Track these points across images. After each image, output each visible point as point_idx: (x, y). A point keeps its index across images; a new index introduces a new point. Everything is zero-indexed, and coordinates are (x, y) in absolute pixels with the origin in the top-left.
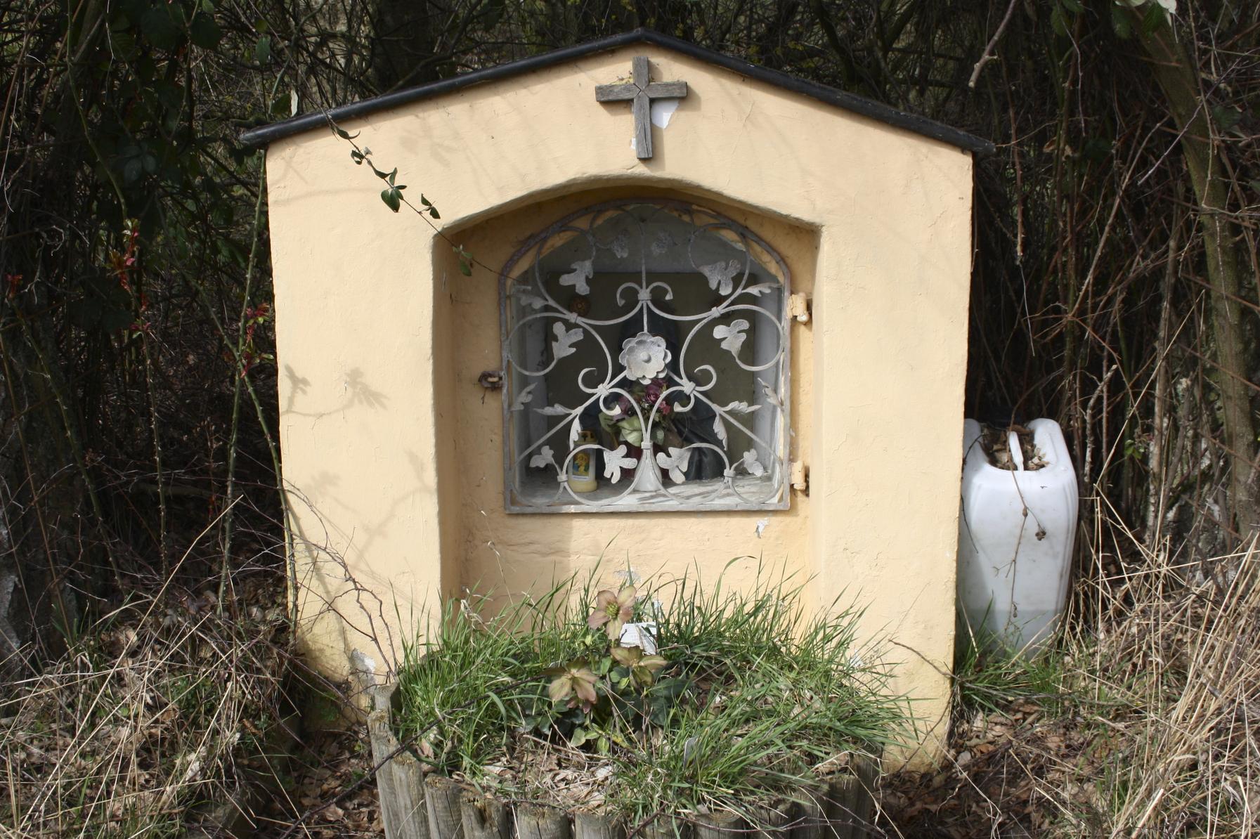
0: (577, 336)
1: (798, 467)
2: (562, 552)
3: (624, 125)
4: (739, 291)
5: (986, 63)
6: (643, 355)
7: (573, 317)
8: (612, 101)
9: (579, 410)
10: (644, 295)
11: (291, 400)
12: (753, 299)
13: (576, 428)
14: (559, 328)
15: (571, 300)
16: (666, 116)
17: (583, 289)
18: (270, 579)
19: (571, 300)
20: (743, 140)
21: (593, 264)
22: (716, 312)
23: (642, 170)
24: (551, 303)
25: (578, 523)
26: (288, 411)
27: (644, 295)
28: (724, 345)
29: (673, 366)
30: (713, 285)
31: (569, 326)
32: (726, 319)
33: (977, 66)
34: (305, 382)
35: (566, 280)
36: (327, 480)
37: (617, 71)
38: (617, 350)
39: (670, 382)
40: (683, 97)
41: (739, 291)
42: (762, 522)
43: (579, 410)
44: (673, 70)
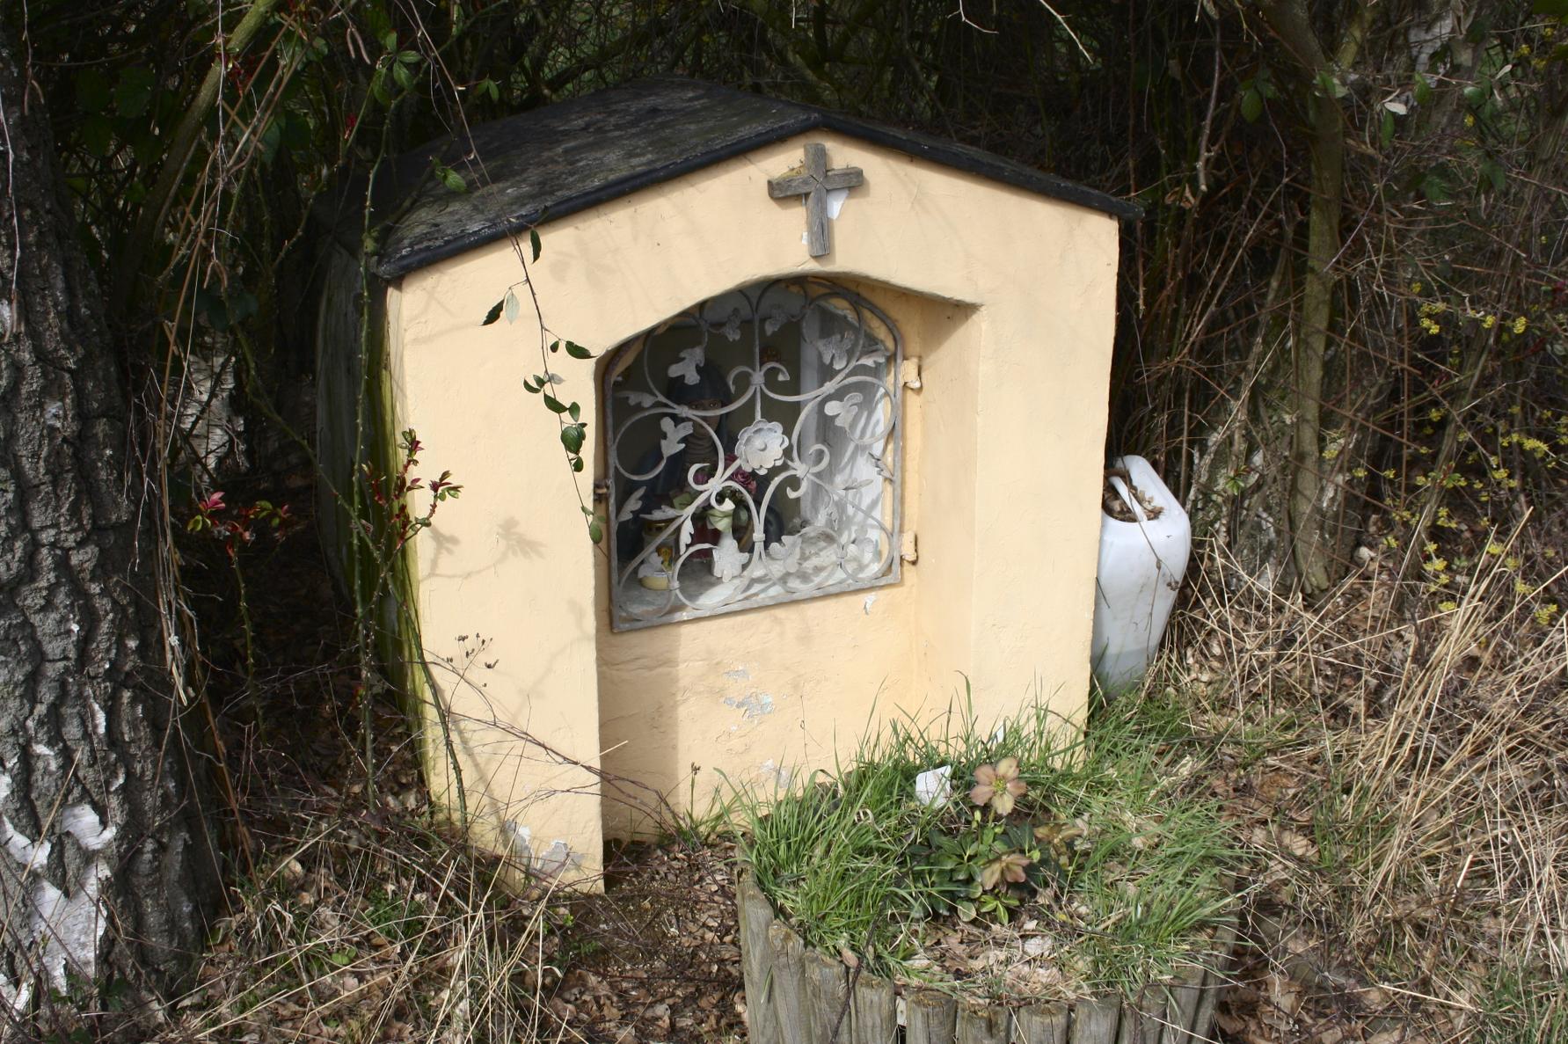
0: (686, 430)
1: (908, 539)
2: (670, 662)
3: (796, 218)
4: (853, 364)
5: (1208, 160)
6: (758, 442)
7: (684, 411)
8: (782, 192)
9: (691, 510)
10: (758, 378)
11: (434, 563)
12: (863, 370)
13: (688, 529)
14: (667, 424)
15: (677, 391)
16: (837, 206)
17: (692, 378)
18: (409, 771)
19: (677, 391)
20: (910, 220)
21: (706, 351)
22: (830, 387)
23: (812, 266)
24: (662, 399)
25: (685, 629)
26: (432, 574)
27: (758, 378)
28: (838, 422)
29: (787, 453)
30: (827, 360)
31: (678, 420)
32: (839, 395)
33: (1200, 165)
34: (454, 540)
35: (674, 371)
36: (474, 646)
37: (785, 161)
38: (730, 443)
39: (785, 467)
40: (854, 182)
41: (853, 364)
42: (869, 598)
43: (691, 510)
44: (844, 155)
